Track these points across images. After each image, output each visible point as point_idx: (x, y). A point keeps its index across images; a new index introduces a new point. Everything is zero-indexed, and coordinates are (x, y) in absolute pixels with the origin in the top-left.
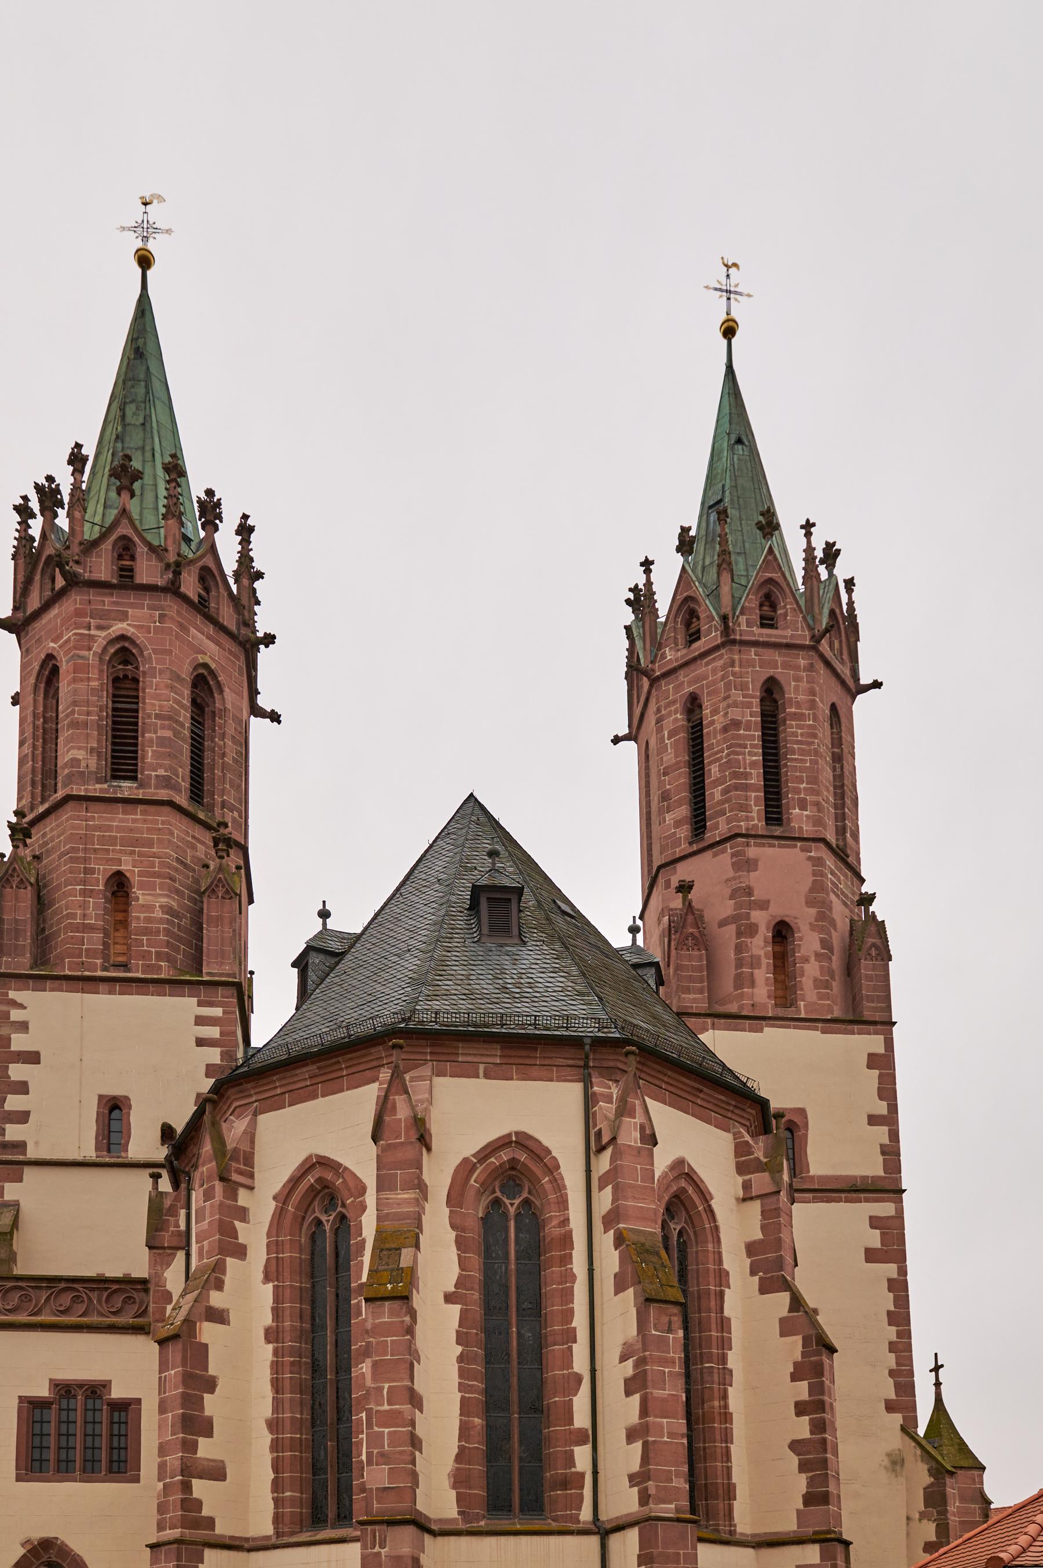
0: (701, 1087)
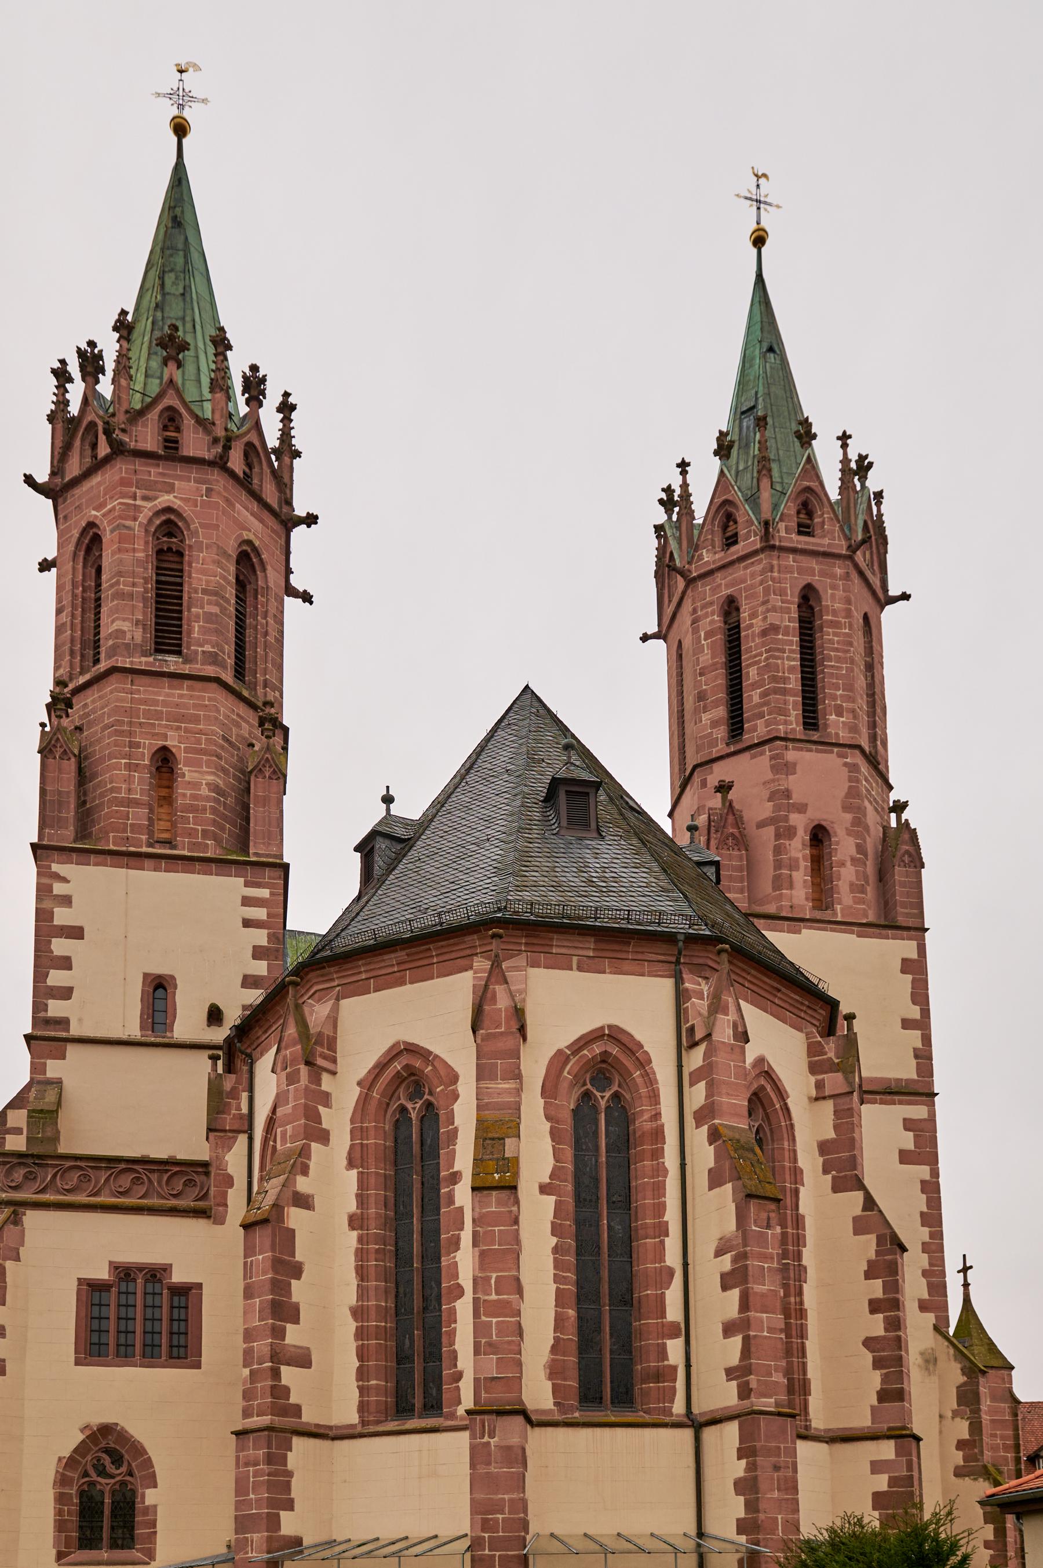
0: (779, 986)
